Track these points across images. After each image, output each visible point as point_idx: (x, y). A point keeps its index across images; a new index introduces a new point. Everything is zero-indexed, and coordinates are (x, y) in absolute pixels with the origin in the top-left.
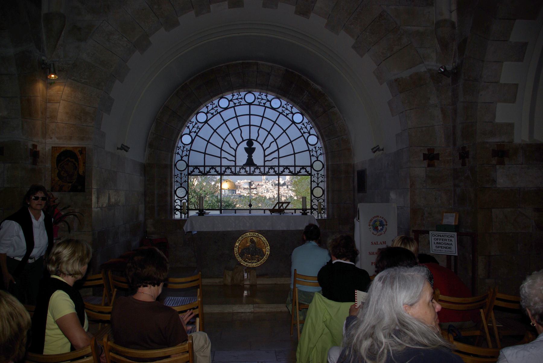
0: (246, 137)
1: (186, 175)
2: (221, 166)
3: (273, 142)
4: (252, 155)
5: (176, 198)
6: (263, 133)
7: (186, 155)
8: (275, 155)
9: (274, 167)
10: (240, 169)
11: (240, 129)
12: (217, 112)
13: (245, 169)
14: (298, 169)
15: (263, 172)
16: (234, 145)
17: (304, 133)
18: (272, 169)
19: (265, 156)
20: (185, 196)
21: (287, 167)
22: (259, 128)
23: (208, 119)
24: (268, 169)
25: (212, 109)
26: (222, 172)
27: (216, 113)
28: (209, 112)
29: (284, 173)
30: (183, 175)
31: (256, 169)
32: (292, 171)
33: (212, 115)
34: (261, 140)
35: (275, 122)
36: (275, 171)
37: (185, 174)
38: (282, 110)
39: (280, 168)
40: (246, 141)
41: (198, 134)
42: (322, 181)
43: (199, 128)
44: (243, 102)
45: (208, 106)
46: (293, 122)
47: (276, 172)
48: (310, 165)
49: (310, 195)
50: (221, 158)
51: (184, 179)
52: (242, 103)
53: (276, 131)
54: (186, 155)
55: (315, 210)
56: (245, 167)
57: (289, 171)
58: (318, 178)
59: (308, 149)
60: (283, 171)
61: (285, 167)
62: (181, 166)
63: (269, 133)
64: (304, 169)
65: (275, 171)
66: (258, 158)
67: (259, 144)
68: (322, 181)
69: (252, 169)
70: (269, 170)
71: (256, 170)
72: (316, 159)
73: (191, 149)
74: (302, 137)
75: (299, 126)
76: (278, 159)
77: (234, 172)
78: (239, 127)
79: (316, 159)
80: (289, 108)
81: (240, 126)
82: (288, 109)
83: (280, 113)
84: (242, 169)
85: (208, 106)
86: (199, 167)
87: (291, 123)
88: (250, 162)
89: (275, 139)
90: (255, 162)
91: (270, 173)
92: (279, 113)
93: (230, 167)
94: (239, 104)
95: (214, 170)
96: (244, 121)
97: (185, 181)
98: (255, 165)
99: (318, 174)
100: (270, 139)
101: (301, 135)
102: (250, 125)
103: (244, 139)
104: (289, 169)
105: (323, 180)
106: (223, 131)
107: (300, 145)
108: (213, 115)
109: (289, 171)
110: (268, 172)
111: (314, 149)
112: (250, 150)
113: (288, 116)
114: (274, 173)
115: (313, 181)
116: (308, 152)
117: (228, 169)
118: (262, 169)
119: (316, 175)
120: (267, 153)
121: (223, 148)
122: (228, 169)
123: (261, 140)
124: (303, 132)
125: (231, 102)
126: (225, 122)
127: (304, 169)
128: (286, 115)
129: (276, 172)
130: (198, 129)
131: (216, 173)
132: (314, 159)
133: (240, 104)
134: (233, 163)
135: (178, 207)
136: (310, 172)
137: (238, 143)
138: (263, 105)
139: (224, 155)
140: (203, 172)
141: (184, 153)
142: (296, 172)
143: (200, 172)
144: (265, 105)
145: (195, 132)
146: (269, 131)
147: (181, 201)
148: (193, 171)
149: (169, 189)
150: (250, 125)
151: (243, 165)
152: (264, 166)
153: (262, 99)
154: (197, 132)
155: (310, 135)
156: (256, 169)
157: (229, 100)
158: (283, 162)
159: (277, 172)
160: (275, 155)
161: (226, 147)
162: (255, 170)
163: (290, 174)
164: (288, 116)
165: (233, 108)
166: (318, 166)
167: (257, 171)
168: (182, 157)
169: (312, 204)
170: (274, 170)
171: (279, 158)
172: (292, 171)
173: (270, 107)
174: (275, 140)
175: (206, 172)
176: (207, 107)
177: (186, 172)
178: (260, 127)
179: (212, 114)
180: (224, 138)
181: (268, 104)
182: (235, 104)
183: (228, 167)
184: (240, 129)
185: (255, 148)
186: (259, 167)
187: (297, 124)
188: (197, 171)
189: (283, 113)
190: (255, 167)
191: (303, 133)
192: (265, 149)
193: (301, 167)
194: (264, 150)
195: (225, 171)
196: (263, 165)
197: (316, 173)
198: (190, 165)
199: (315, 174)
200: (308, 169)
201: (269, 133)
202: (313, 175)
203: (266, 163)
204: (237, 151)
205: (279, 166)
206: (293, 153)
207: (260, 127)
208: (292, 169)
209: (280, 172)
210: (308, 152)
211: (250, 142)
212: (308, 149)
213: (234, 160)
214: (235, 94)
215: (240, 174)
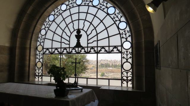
0: (76, 27)
4: (80, 40)
5: (36, 68)
6: (87, 24)
8: (95, 39)
10: (72, 49)
13: (75, 49)
14: (111, 48)
15: (87, 51)
16: (69, 34)
17: (116, 21)
19: (88, 40)
20: (41, 67)
21: (103, 47)
22: (84, 21)
26: (62, 52)
29: (101, 52)
34: (85, 29)
35: (95, 16)
36: (95, 51)
38: (100, 6)
39: (98, 48)
41: (49, 29)
46: (108, 14)
48: (120, 45)
49: (121, 68)
50: (61, 42)
52: (74, 6)
53: (96, 22)
55: (124, 80)
58: (127, 55)
59: (119, 33)
60: (101, 50)
62: (40, 48)
63: (91, 23)
64: (116, 49)
65: (95, 51)
66: (83, 42)
69: (80, 49)
70: (90, 50)
71: (82, 50)
72: (126, 40)
73: (45, 38)
74: (115, 24)
75: (112, 16)
79: (125, 40)
82: (104, 5)
83: (99, 9)
88: (78, 45)
89: (95, 27)
90: (82, 44)
92: (98, 9)
96: (75, 17)
97: (41, 58)
99: (127, 52)
100: (92, 28)
101: (114, 23)
104: (105, 49)
106: (63, 25)
107: (113, 30)
110: (90, 51)
111: (124, 33)
112: (78, 37)
113: (104, 10)
114: (94, 52)
118: (86, 49)
119: (126, 53)
120: (89, 37)
121: (62, 36)
123: (85, 29)
125: (68, 6)
127: (116, 49)
131: (58, 53)
132: (124, 40)
134: (68, 46)
135: (37, 74)
137: (71, 32)
139: (63, 40)
140: (51, 52)
142: (110, 51)
143: (49, 52)
145: (48, 27)
147: (39, 70)
148: (46, 52)
149: (27, 63)
155: (121, 22)
158: (101, 44)
159: (96, 51)
160: (95, 39)
161: (64, 36)
162: (81, 50)
163: (105, 52)
164: (104, 10)
166: (127, 45)
167: (83, 51)
168: (40, 43)
171: (98, 41)
173: (92, 5)
174: (95, 28)
177: (42, 52)
178: (85, 20)
179: (57, 15)
182: (70, 7)
183: (65, 49)
187: (110, 15)
188: (47, 52)
189: (101, 8)
194: (88, 36)
196: (87, 46)
197: (125, 51)
198: (44, 48)
199: (124, 52)
200: (119, 48)
201: (91, 23)
202: (123, 53)
205: (97, 47)
208: (107, 49)
211: (79, 31)
212: (119, 33)
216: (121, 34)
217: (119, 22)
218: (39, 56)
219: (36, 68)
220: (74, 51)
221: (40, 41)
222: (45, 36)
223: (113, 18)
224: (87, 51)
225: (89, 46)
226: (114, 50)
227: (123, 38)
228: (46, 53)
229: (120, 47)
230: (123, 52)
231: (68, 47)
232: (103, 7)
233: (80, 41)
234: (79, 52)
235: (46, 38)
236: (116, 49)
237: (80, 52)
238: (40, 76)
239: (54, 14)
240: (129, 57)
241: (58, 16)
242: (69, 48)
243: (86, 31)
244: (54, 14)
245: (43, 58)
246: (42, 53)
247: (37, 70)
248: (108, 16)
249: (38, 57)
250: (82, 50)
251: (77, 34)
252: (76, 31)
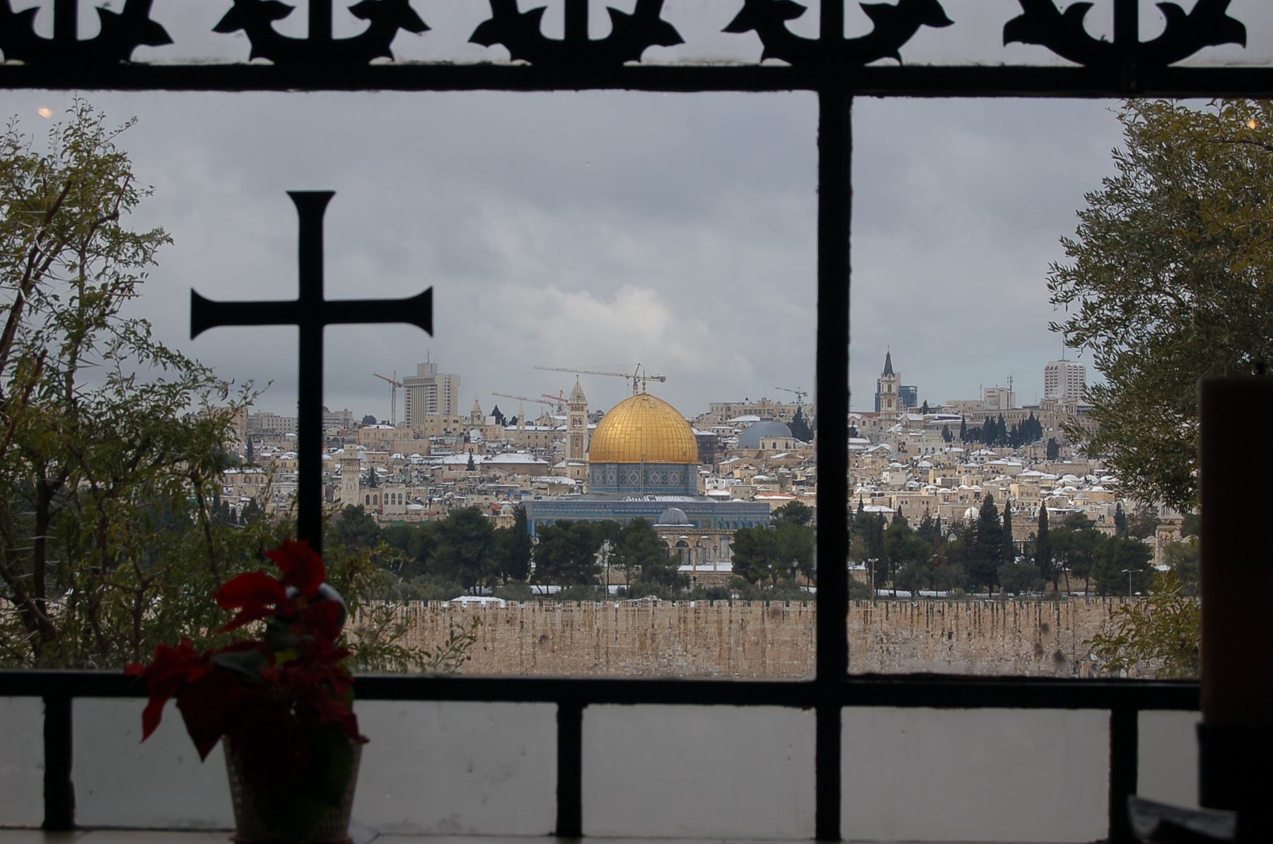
47: (792, 26)
77: (44, 27)
91: (670, 37)
129: (792, 26)
215: (143, 54)
224: (553, 27)
237: (378, 40)
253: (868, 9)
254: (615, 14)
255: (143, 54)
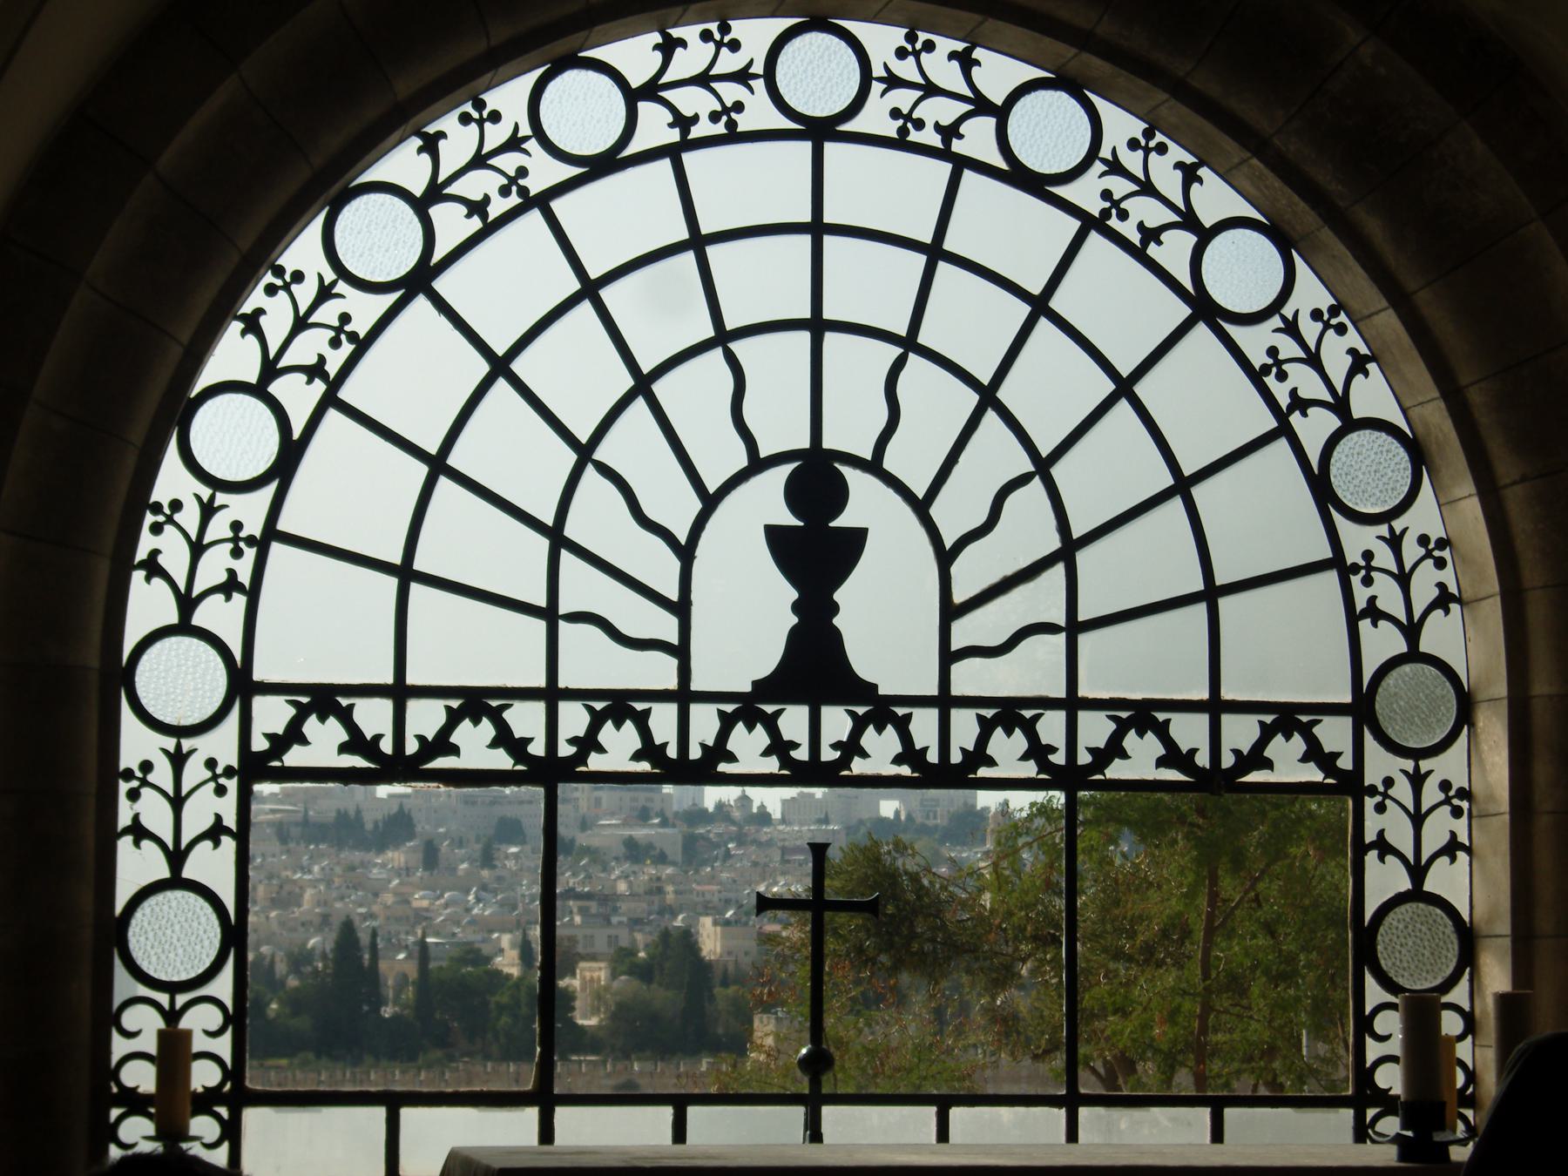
1: (229, 772)
2: (552, 695)
3: (1021, 481)
7: (230, 586)
9: (1028, 714)
10: (727, 723)
11: (732, 361)
12: (523, 191)
13: (771, 724)
14: (1240, 732)
15: (933, 757)
16: (678, 511)
17: (1300, 404)
18: (1009, 733)
19: (950, 611)
22: (893, 352)
23: (439, 254)
24: (978, 730)
25: (479, 161)
26: (565, 750)
27: (514, 200)
28: (448, 191)
30: (194, 771)
31: (871, 730)
32: (1193, 751)
33: (476, 224)
36: (1037, 751)
37: (211, 764)
38: (1106, 195)
39: (1084, 717)
40: (786, 470)
41: (344, 394)
42: (1452, 848)
43: (353, 337)
44: (759, 113)
45: (441, 135)
46: (1204, 309)
47: (1054, 758)
50: (550, 614)
51: (203, 810)
52: (745, 123)
54: (230, 586)
55: (1388, 1104)
56: (769, 709)
57: (1161, 751)
59: (1329, 554)
61: (1124, 715)
63: (988, 397)
65: (1037, 751)
67: (897, 499)
68: (1452, 848)
69: (837, 722)
70: (983, 740)
71: (869, 738)
73: (271, 533)
74: (1282, 444)
75: (1256, 341)
76: (1063, 636)
77: (672, 752)
78: (723, 337)
80: (1168, 180)
81: (730, 324)
83: (1090, 224)
84: (740, 727)
85: (441, 135)
86: (344, 702)
87: (1185, 311)
89: (1045, 451)
90: (865, 659)
91: (991, 762)
92: (1074, 225)
93: (639, 706)
94: (720, 129)
95: (487, 729)
97: (215, 832)
98: (864, 691)
99: (1417, 780)
101: (1272, 423)
102: (817, 326)
103: (763, 454)
104: (1162, 731)
105: (1463, 838)
108: (484, 215)
109: (1161, 751)
115: (1372, 846)
116: (1331, 578)
117: (618, 725)
118: (924, 727)
119: (1403, 791)
120: (969, 576)
121: (570, 531)
122: (618, 725)
124: (1284, 401)
126: (590, 290)
128: (1135, 238)
130: (347, 348)
131: (502, 760)
133: (731, 124)
134: (660, 672)
135: (141, 1077)
136: (1345, 763)
137: (712, 488)
138: (936, 141)
140: (387, 746)
141: (214, 566)
143: (357, 742)
144: (957, 146)
145: (315, 371)
146: (985, 378)
148: (294, 735)
150: (817, 326)
151: (748, 688)
152: (945, 701)
153: (930, 90)
154: (332, 369)
156: (871, 730)
157: (636, 80)
159: (1059, 758)
162: (857, 732)
164: (1153, 250)
165: (665, 165)
167: (881, 749)
169: (1370, 1057)
170: (1032, 735)
171: (1074, 628)
172: (1193, 751)
174: (1043, 466)
175: (412, 747)
176: (430, 146)
177: (222, 745)
178: (909, 343)
179: (477, 208)
180: (584, 438)
181: (978, 139)
182: (683, 122)
184: (732, 361)
185: (867, 529)
186: (901, 711)
187: (1232, 330)
189: (1114, 222)
190: (861, 710)
191: (1291, 409)
192: (948, 544)
193: (1269, 719)
194: (946, 557)
195: (588, 743)
196: (932, 690)
199: (1389, 782)
200: (1335, 734)
201: (988, 397)
202: (1372, 790)
203: (959, 670)
204: (701, 551)
205: (1073, 704)
206: (1198, 585)
207: (909, 343)
209: (1084, 758)
210: (1331, 578)
212: (1326, 553)
213: (674, 639)
214: (690, 33)
215: (723, 767)
216: (1355, 568)
217: (1333, 422)
218: (177, 802)
219: (124, 985)
220: (748, 747)
221: (175, 557)
222: (270, 490)
223: (1266, 369)
224: (933, 757)
225: (956, 690)
226: (1268, 753)
227: (1374, 613)
228: (295, 757)
229: (1345, 724)
230: (1372, 777)
231: (672, 683)
232: (1148, 212)
233: (835, 609)
234: (828, 755)
235: (283, 525)
236: (1298, 744)
238: (205, 1102)
239: (418, 188)
240: (1447, 837)
241: (489, 229)
242: (684, 696)
243: (920, 493)
244: (418, 190)
245: (242, 836)
246: (229, 756)
247: (145, 1023)
248: (1201, 331)
249: (154, 812)
250: (869, 738)
251: (792, 521)
252: (784, 471)
253: (1091, 750)
254: (963, 750)
255: (723, 767)
